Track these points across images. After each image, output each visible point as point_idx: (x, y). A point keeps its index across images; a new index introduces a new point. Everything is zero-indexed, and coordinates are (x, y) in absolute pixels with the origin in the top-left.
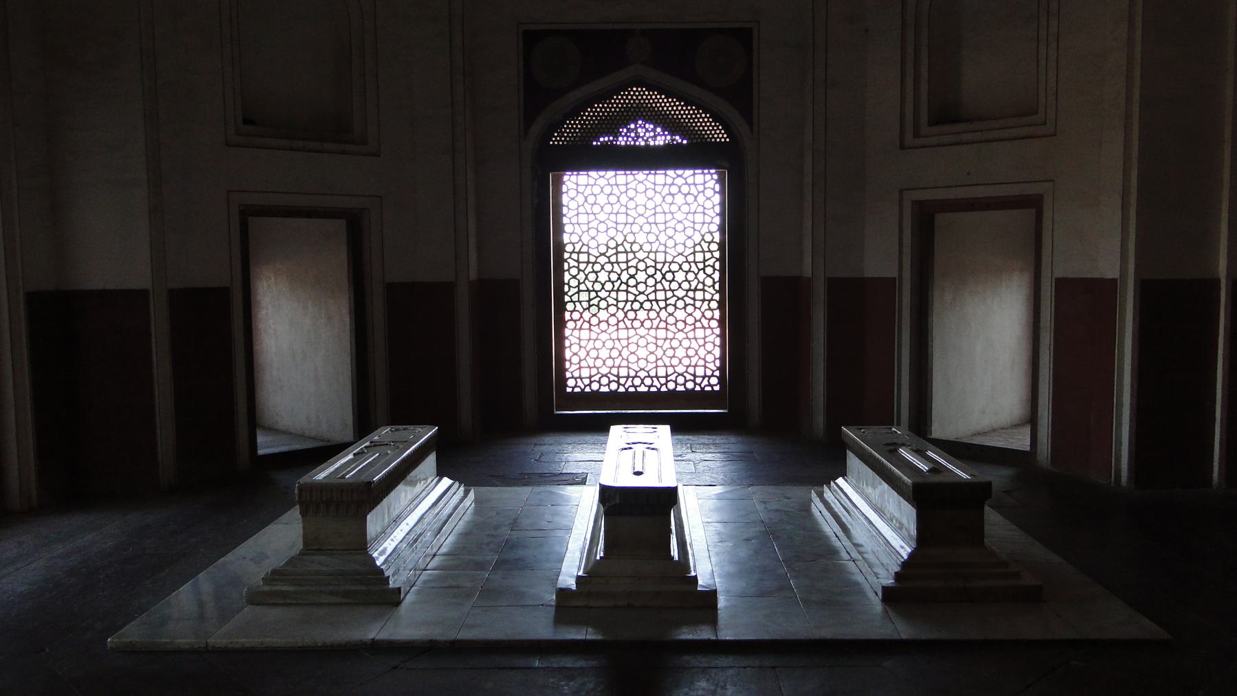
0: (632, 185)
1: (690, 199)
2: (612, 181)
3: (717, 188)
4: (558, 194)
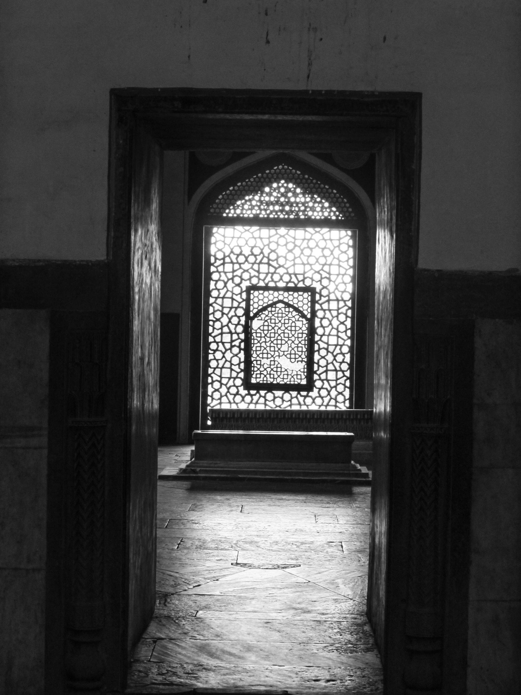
0: (274, 239)
2: (256, 234)
3: (351, 243)
4: (208, 244)
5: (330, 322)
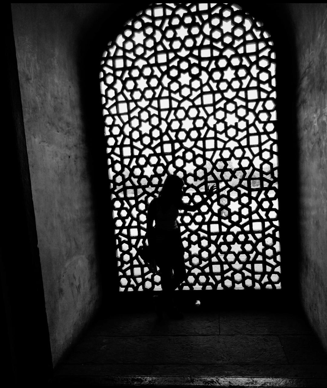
1: (242, 73)
3: (273, 56)
5: (251, 161)
